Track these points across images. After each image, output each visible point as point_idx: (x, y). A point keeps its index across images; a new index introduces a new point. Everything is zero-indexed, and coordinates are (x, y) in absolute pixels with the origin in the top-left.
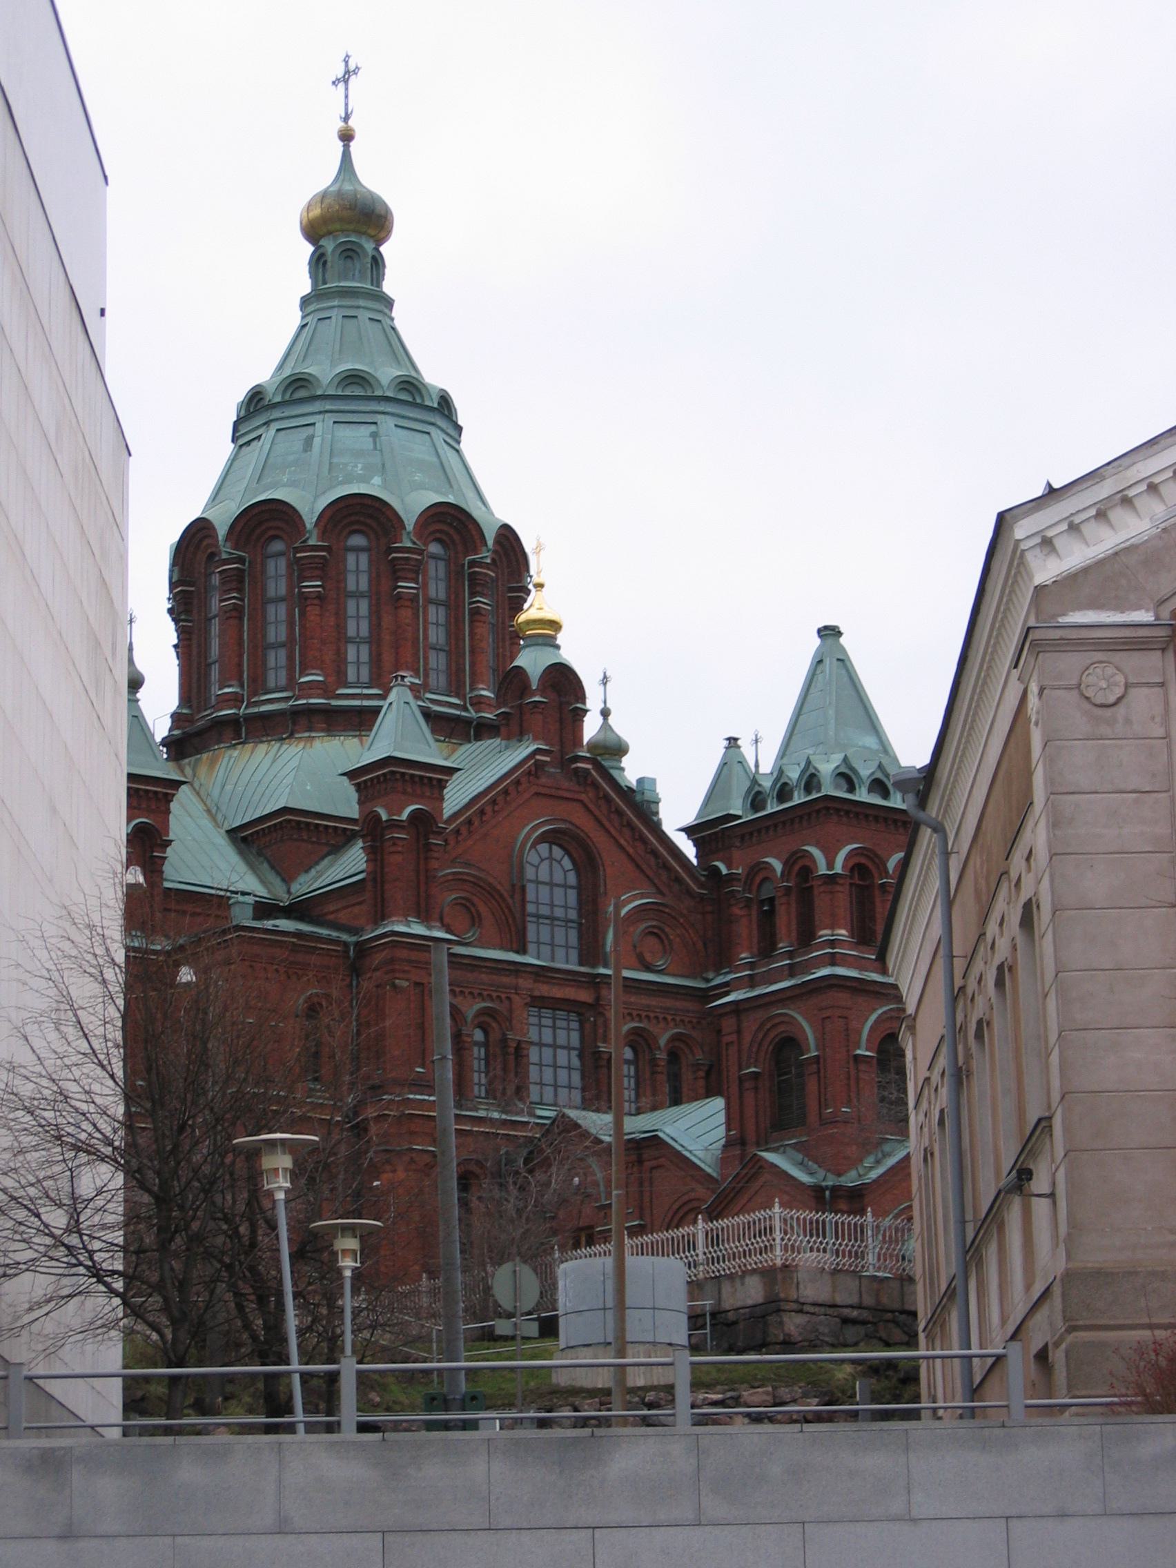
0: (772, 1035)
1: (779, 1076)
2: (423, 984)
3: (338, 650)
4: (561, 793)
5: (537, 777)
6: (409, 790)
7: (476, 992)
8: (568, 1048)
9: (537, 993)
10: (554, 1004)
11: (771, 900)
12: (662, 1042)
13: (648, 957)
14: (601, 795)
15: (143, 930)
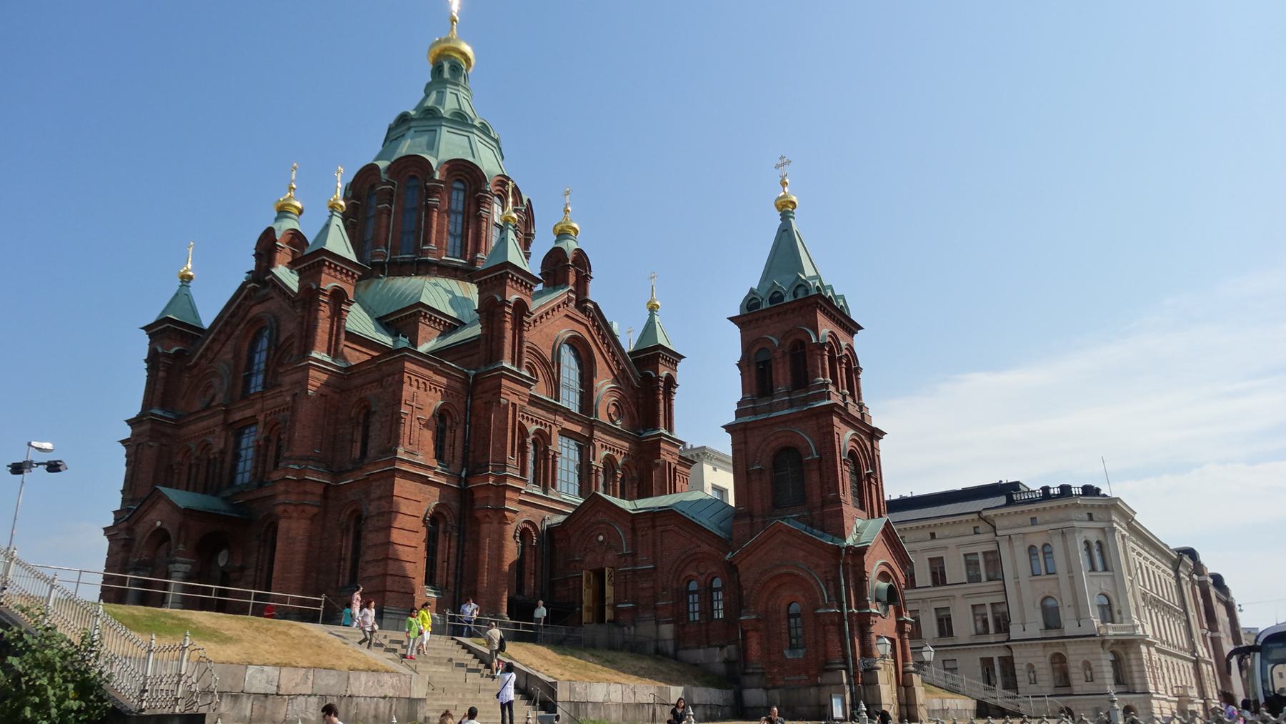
1: (775, 472)
5: (567, 306)
6: (515, 286)
9: (563, 426)
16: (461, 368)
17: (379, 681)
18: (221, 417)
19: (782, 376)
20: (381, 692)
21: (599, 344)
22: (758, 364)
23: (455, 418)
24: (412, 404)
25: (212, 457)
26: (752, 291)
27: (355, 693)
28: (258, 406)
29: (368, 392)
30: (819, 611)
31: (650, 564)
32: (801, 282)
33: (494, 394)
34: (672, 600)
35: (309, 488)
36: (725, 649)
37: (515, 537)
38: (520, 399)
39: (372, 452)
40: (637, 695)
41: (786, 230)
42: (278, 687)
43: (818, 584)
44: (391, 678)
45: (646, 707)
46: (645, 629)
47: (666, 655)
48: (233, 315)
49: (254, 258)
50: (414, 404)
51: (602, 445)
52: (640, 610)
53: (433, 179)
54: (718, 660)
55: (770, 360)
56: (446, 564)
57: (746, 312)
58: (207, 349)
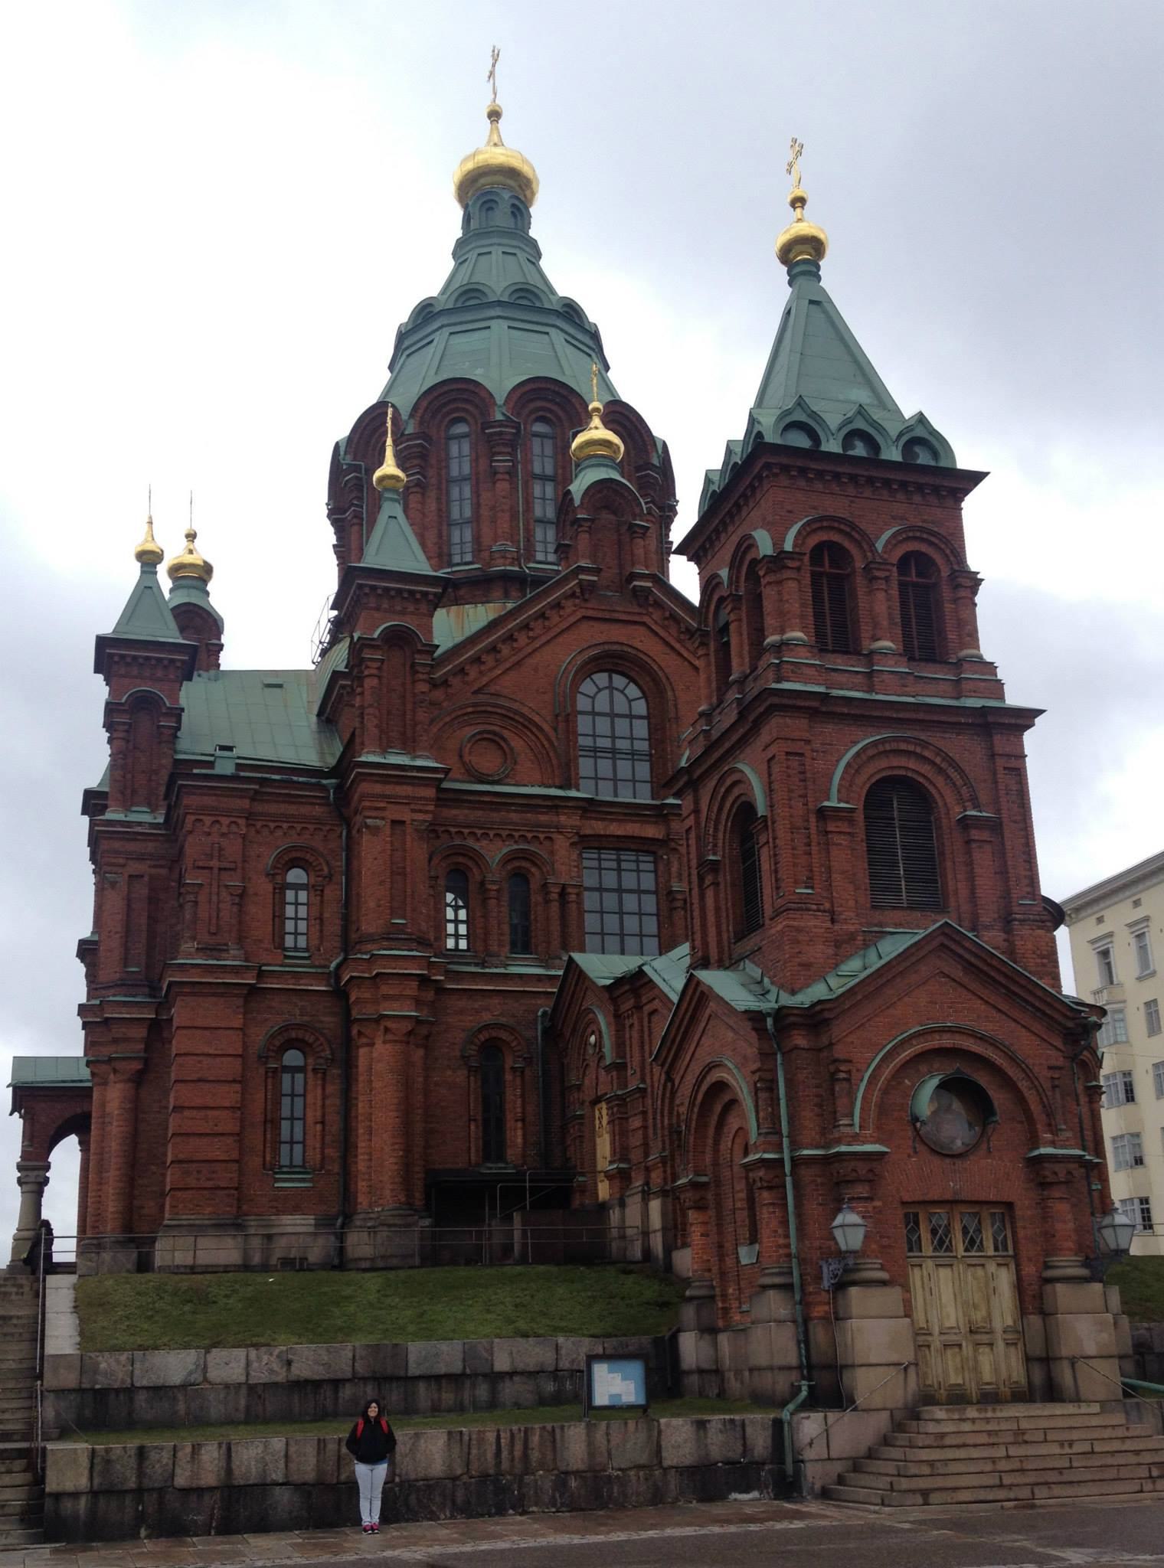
2: (403, 822)
4: (616, 616)
7: (504, 833)
10: (621, 844)
14: (667, 614)
15: (149, 805)
16: (313, 780)
23: (322, 870)
24: (211, 864)
35: (118, 1031)
37: (463, 1057)
38: (413, 811)
50: (214, 863)
56: (319, 1127)
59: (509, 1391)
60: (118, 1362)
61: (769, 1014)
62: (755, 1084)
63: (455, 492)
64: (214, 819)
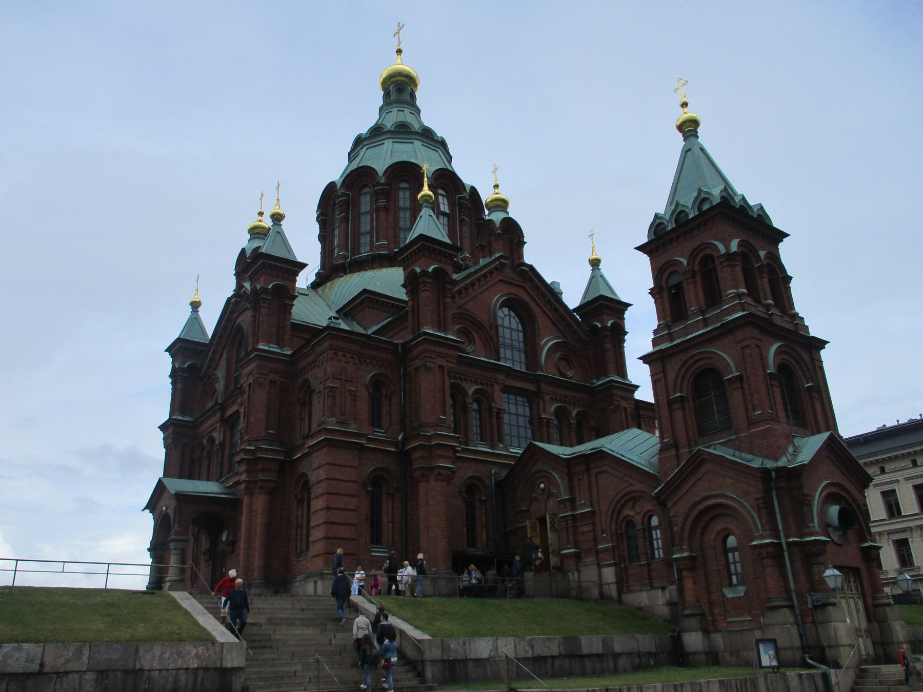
0: (692, 369)
2: (444, 366)
3: (395, 233)
5: (501, 271)
7: (474, 379)
8: (524, 416)
9: (506, 384)
11: (678, 286)
12: (574, 414)
13: (563, 370)
14: (534, 284)
17: (179, 653)
18: (219, 414)
19: (694, 297)
20: (180, 663)
21: (541, 304)
22: (670, 289)
25: (215, 449)
26: (657, 216)
27: (147, 667)
28: (239, 400)
29: (309, 374)
30: (754, 543)
31: (588, 507)
32: (703, 196)
33: (420, 360)
34: (612, 542)
36: (667, 589)
38: (448, 361)
39: (314, 427)
40: (535, 647)
41: (689, 150)
42: (42, 665)
43: (750, 514)
44: (195, 647)
45: (549, 660)
46: (589, 574)
47: (610, 599)
48: (225, 329)
49: (235, 277)
50: (343, 377)
51: (551, 398)
52: (583, 555)
53: (379, 184)
54: (661, 602)
55: (681, 283)
56: (390, 524)
57: (653, 237)
58: (212, 360)
59: (622, 662)
60: (459, 644)
61: (773, 470)
62: (758, 505)
63: (401, 214)
64: (343, 353)
